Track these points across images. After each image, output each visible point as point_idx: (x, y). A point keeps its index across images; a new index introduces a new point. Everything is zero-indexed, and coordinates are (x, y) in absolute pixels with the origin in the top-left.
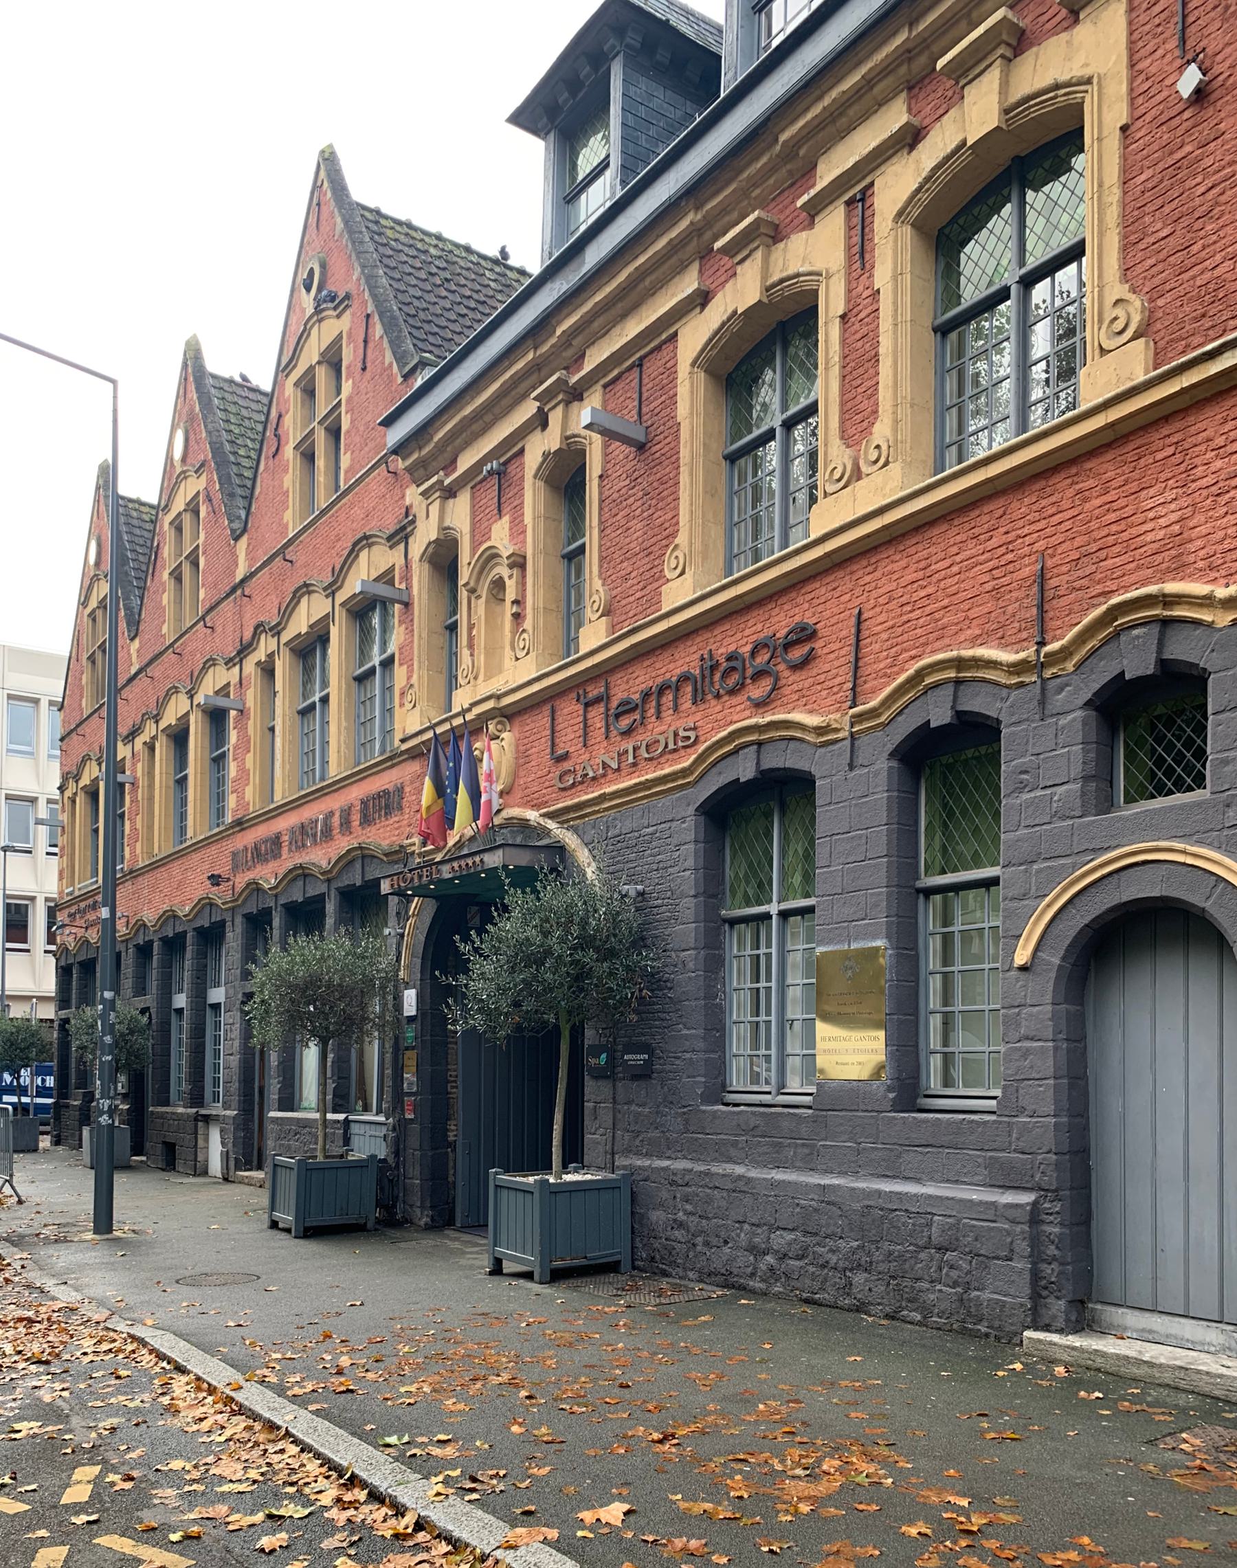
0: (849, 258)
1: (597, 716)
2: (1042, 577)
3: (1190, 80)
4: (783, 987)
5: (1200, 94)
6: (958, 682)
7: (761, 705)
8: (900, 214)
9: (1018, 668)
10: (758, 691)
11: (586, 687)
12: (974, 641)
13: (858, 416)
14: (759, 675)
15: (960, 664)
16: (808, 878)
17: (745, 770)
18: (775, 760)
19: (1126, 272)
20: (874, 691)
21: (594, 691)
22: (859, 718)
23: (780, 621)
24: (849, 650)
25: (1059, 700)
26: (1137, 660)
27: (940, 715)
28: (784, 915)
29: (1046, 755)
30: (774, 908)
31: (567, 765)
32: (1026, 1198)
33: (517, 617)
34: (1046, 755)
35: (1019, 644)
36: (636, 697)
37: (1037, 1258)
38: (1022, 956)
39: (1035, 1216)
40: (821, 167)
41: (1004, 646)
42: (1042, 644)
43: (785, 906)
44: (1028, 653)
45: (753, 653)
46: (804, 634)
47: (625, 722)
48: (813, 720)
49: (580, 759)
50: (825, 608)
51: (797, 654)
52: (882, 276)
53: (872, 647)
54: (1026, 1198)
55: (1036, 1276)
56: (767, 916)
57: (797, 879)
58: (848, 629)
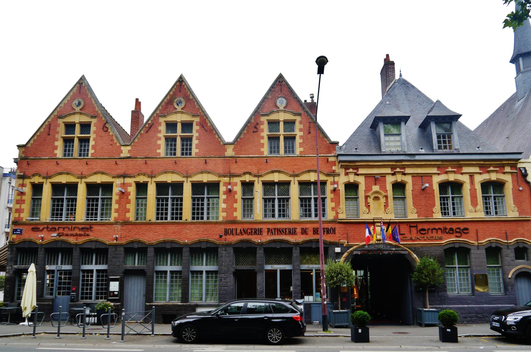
1: (414, 230)
2: (506, 233)
7: (457, 237)
10: (458, 235)
11: (412, 224)
14: (457, 232)
17: (457, 246)
19: (514, 204)
21: (412, 225)
23: (462, 226)
24: (475, 234)
25: (510, 247)
26: (521, 246)
29: (509, 255)
31: (404, 236)
33: (386, 206)
34: (509, 255)
36: (426, 228)
38: (510, 276)
44: (506, 241)
47: (422, 232)
49: (408, 236)
53: (479, 234)
56: (456, 267)
58: (475, 231)
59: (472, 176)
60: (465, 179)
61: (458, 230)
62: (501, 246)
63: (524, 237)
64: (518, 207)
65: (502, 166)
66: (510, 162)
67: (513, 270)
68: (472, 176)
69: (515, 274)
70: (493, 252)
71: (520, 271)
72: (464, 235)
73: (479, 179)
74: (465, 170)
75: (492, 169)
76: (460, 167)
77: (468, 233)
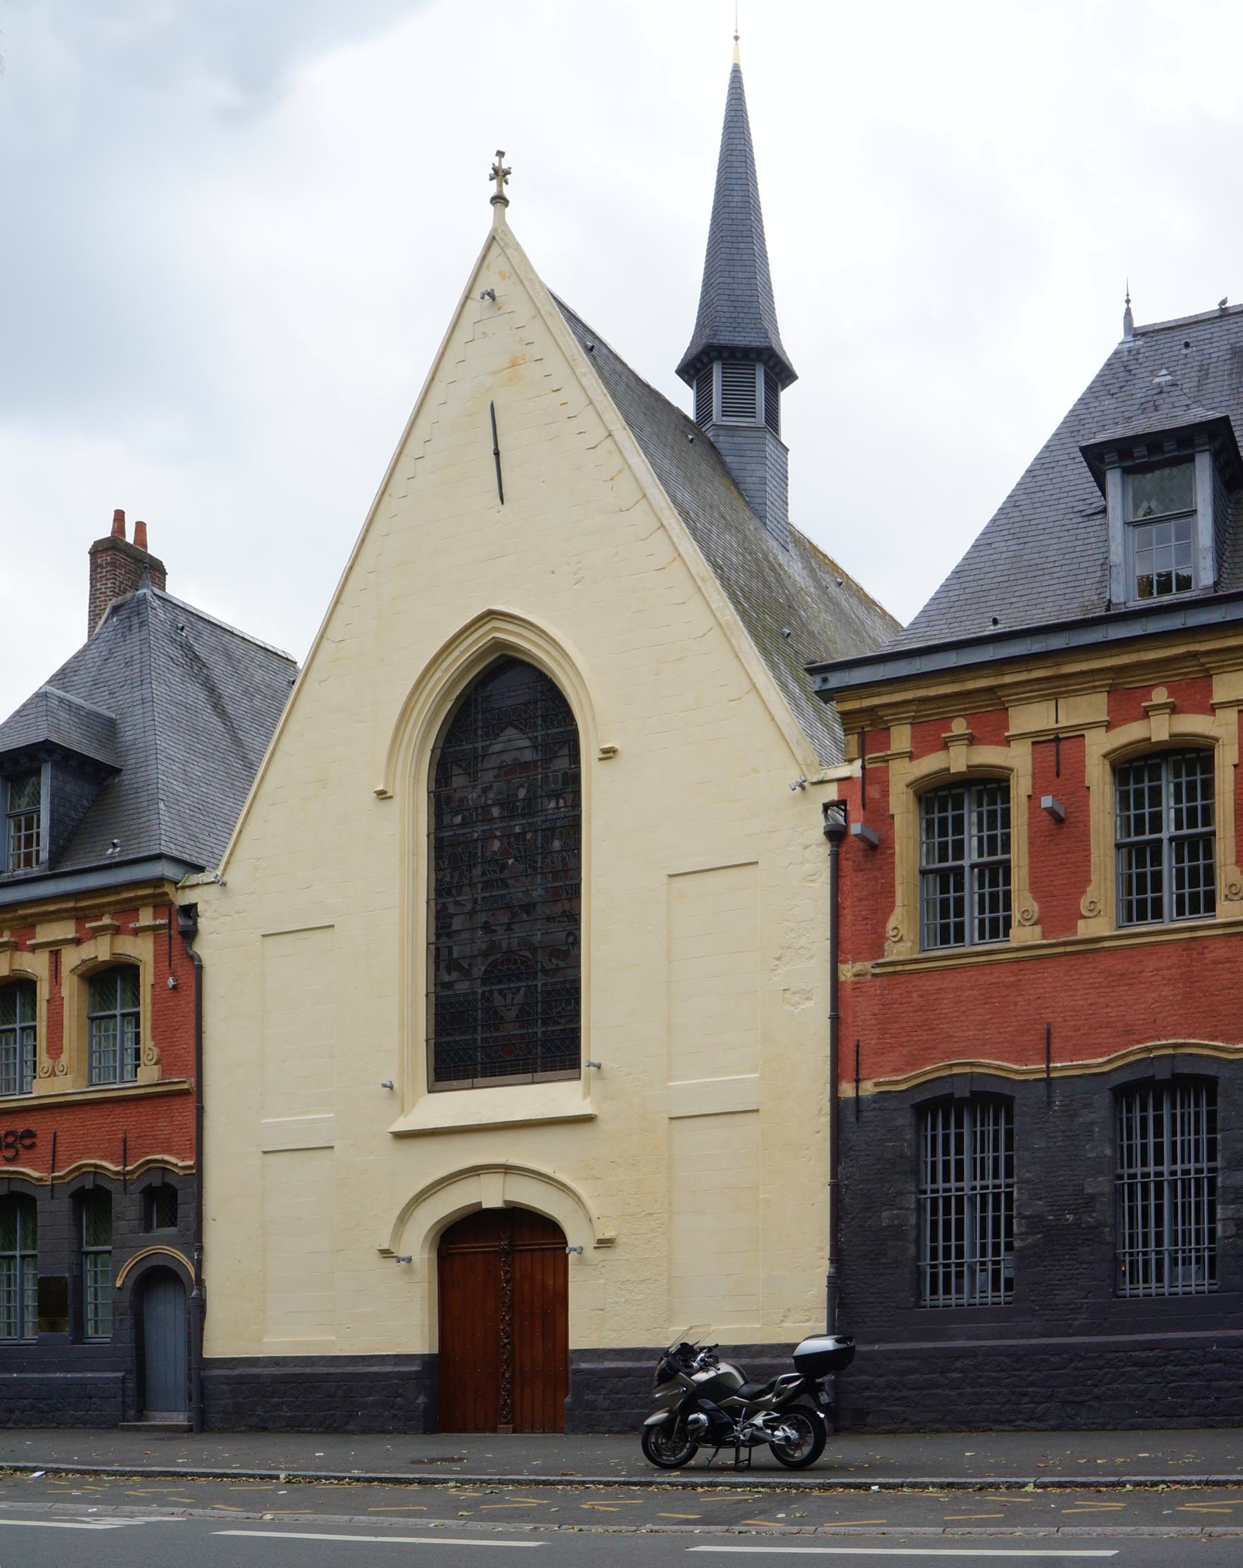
0: (51, 976)
2: (125, 1141)
3: (171, 982)
4: (22, 1291)
5: (174, 987)
6: (95, 1173)
8: (72, 970)
9: (117, 1173)
10: (10, 1153)
12: (102, 1158)
13: (55, 1049)
14: (8, 1146)
15: (96, 1166)
16: (34, 1241)
18: (16, 1187)
20: (64, 1167)
22: (54, 1178)
23: (20, 1125)
25: (131, 1188)
26: (156, 1181)
27: (89, 1185)
28: (23, 1257)
29: (127, 1208)
30: (18, 1253)
32: (120, 1374)
34: (127, 1208)
35: (117, 1165)
37: (124, 1395)
39: (123, 1380)
40: (38, 929)
41: (112, 1162)
42: (125, 1166)
43: (24, 1253)
44: (119, 1168)
45: (6, 1135)
46: (29, 1134)
48: (36, 1174)
50: (43, 1127)
51: (27, 1142)
52: (65, 991)
54: (120, 1374)
55: (124, 1403)
56: (15, 1257)
57: (29, 1241)
58: (51, 1138)
59: (55, 950)
60: (35, 965)
61: (10, 1140)
62: (108, 1186)
63: (168, 1151)
64: (162, 1050)
65: (130, 909)
66: (140, 893)
67: (130, 1263)
68: (55, 950)
69: (135, 1274)
70: (92, 1200)
71: (147, 1264)
72: (24, 1154)
73: (71, 958)
74: (46, 933)
75: (106, 920)
76: (30, 925)
77: (33, 1146)
